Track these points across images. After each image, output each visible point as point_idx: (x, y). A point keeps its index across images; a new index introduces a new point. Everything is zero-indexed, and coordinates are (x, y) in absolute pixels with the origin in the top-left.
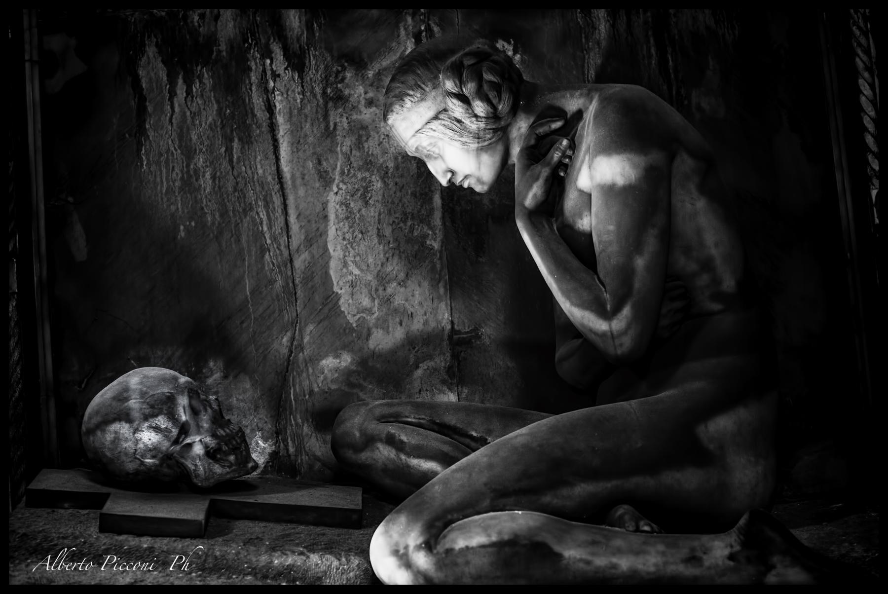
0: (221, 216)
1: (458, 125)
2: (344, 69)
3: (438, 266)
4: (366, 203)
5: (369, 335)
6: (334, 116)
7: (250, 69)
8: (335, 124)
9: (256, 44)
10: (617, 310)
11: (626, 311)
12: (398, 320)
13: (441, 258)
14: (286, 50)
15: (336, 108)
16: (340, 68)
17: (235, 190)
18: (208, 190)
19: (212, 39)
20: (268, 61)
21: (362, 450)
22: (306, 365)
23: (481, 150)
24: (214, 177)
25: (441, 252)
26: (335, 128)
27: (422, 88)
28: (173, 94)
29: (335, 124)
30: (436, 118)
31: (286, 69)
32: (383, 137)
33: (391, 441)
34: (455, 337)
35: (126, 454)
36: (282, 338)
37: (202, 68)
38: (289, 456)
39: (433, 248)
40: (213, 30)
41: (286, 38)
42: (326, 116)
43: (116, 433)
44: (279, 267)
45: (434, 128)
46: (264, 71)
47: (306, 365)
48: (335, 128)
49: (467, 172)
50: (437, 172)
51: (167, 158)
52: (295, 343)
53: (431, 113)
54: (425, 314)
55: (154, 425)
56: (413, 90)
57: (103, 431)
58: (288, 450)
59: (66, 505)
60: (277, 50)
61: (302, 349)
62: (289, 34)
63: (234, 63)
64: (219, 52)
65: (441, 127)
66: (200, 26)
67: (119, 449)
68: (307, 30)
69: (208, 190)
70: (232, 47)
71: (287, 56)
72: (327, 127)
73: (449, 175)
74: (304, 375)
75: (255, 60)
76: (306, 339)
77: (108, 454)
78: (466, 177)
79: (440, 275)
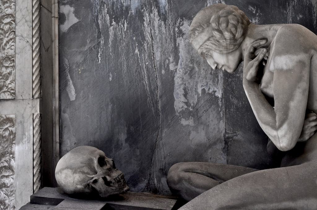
0: (130, 82)
1: (218, 43)
2: (183, 20)
3: (220, 105)
4: (191, 77)
5: (190, 133)
6: (178, 40)
7: (144, 21)
8: (179, 44)
10: (281, 126)
11: (285, 126)
12: (202, 127)
13: (222, 101)
14: (159, 12)
15: (179, 37)
16: (181, 20)
17: (136, 71)
18: (125, 72)
19: (128, 8)
21: (178, 184)
22: (163, 146)
23: (228, 54)
24: (128, 66)
25: (222, 99)
27: (202, 27)
29: (179, 44)
30: (208, 40)
31: (159, 20)
33: (189, 181)
34: (227, 135)
36: (154, 134)
38: (155, 184)
39: (218, 97)
40: (129, 4)
41: (159, 7)
42: (175, 40)
44: (153, 104)
45: (207, 44)
47: (163, 146)
48: (179, 45)
50: (210, 64)
51: (109, 58)
52: (159, 137)
53: (206, 38)
54: (214, 125)
55: (82, 171)
56: (199, 28)
57: (61, 172)
58: (154, 183)
59: (47, 203)
60: (155, 12)
61: (162, 139)
62: (160, 6)
65: (210, 44)
66: (124, 2)
68: (168, 3)
69: (125, 72)
71: (159, 15)
72: (175, 44)
73: (216, 65)
74: (162, 150)
75: (146, 16)
76: (164, 135)
77: (63, 183)
78: (223, 66)
79: (221, 108)
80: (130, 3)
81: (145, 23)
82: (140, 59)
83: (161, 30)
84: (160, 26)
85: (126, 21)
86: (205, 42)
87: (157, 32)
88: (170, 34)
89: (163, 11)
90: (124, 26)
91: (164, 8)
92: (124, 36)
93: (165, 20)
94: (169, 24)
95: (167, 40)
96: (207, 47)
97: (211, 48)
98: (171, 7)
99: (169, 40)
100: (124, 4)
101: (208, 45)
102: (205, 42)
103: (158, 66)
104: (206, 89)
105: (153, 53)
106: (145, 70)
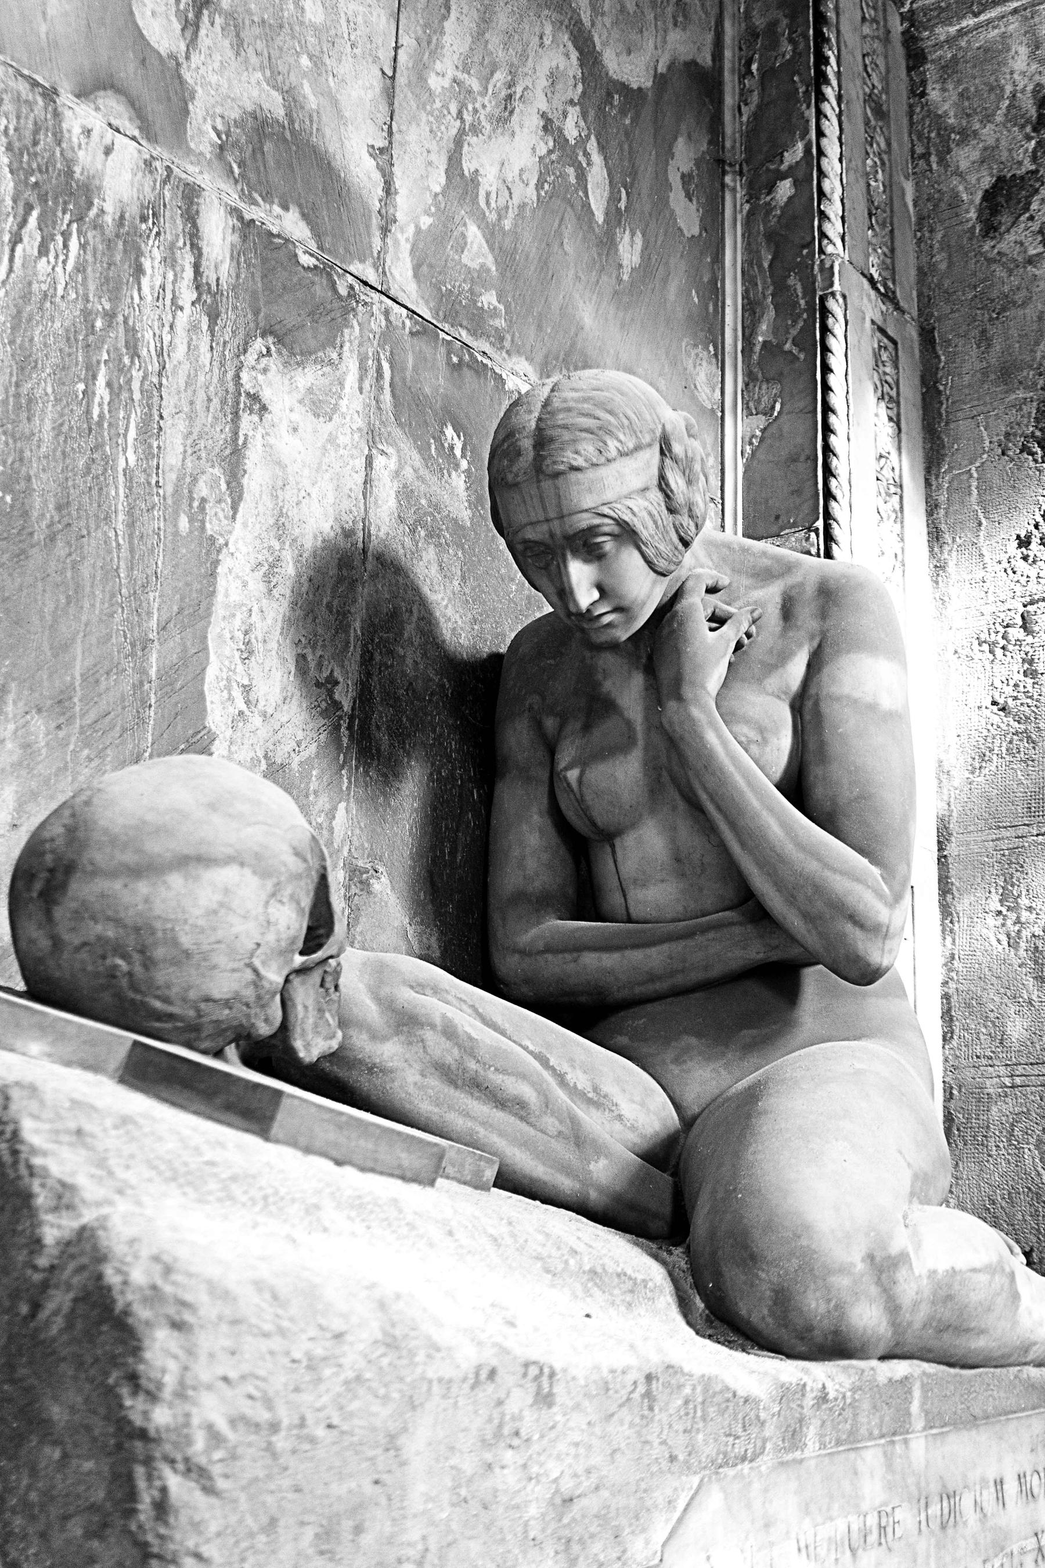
9: (158, 234)
20: (170, 276)
26: (245, 443)
28: (16, 239)
32: (303, 493)
35: (232, 952)
37: (71, 222)
43: (226, 891)
45: (635, 509)
46: (163, 288)
49: (625, 603)
53: (637, 483)
59: (35, 1048)
63: (120, 245)
64: (102, 211)
67: (220, 934)
68: (232, 257)
69: (43, 449)
70: (122, 217)
80: (104, 165)
81: (145, 282)
82: (110, 425)
83: (197, 347)
84: (194, 328)
85: (79, 232)
86: (628, 497)
87: (181, 351)
88: (222, 381)
89: (209, 276)
90: (66, 246)
91: (216, 267)
92: (60, 292)
93: (214, 316)
94: (225, 343)
95: (209, 400)
96: (627, 517)
97: (639, 527)
98: (238, 276)
99: (216, 401)
100: (81, 154)
101: (634, 514)
102: (628, 497)
103: (170, 489)
104: (310, 658)
105: (160, 429)
106: (121, 478)
